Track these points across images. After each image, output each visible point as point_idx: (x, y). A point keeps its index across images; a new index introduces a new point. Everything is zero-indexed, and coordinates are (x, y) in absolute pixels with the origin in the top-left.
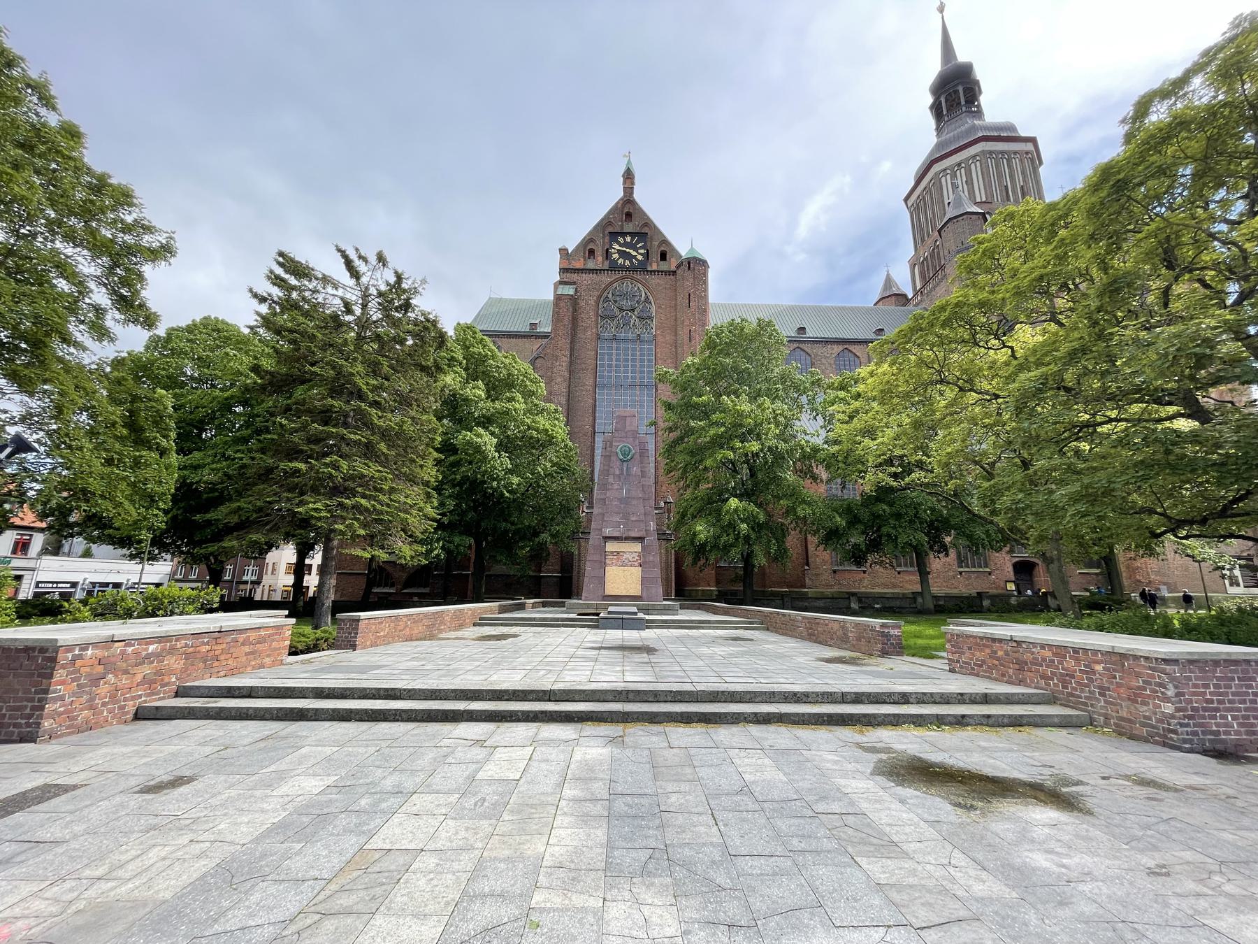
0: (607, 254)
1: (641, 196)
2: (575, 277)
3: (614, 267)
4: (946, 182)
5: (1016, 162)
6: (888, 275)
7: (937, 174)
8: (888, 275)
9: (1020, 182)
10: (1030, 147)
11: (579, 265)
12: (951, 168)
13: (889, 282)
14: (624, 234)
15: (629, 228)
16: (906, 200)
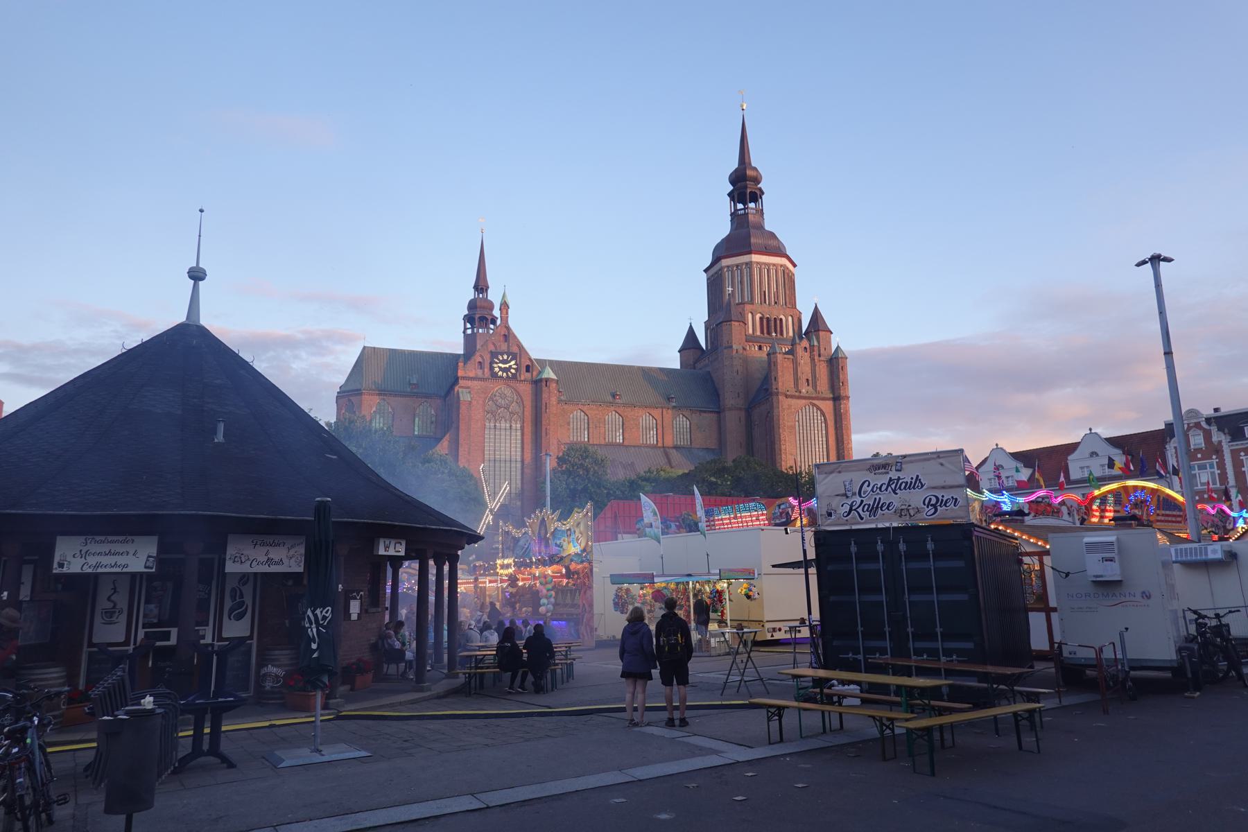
0: (492, 368)
1: (512, 323)
2: (469, 383)
3: (494, 375)
4: (727, 275)
5: (773, 272)
6: (691, 327)
7: (721, 269)
8: (691, 327)
9: (774, 289)
10: (784, 261)
11: (472, 375)
12: (732, 266)
13: (691, 334)
14: (502, 354)
15: (504, 347)
16: (706, 271)
